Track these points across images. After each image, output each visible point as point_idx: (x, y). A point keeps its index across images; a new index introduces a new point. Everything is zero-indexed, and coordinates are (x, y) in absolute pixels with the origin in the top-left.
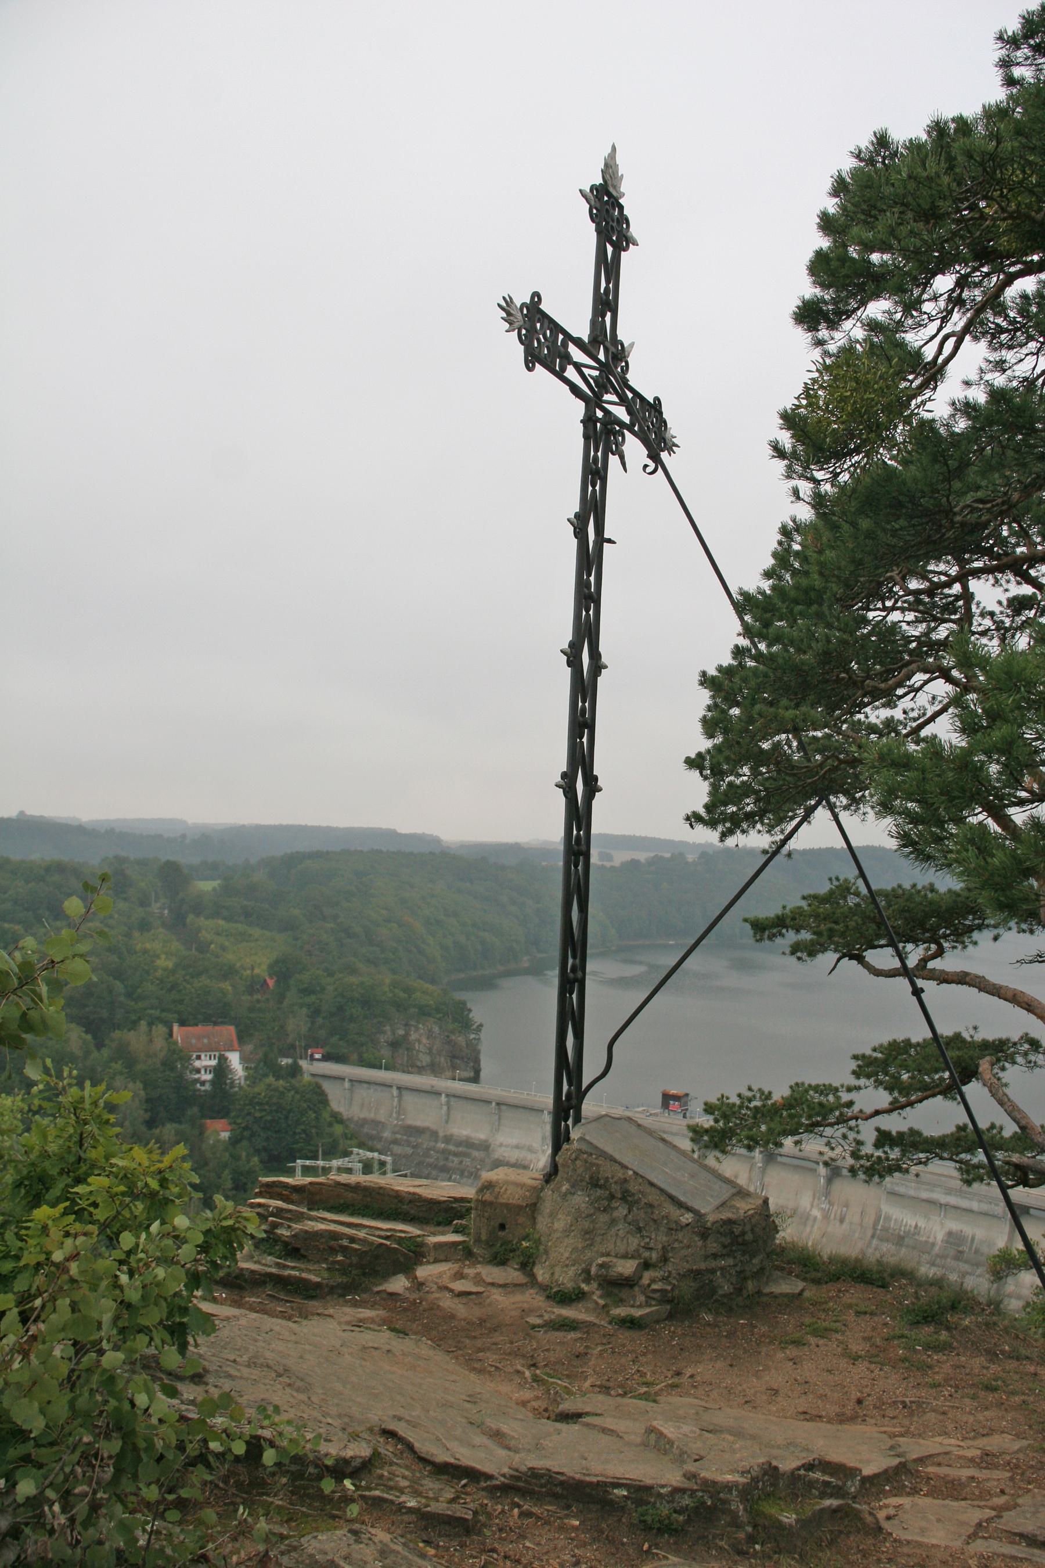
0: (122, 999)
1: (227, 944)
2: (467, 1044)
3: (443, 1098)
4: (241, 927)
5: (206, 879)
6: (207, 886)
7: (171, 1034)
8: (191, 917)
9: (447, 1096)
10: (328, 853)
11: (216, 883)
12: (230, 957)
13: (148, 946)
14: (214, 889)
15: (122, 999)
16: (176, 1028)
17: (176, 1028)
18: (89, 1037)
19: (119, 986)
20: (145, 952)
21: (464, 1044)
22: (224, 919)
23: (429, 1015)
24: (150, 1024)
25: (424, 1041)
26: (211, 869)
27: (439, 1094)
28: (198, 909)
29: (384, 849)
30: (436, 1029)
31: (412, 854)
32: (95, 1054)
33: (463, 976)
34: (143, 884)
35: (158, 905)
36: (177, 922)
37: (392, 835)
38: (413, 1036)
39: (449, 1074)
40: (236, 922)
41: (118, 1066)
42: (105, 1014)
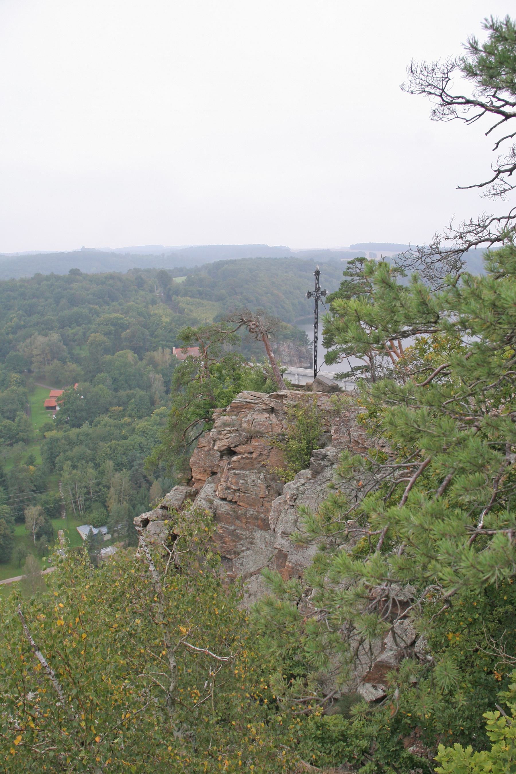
0: (149, 337)
1: (192, 309)
2: (306, 352)
3: (296, 376)
4: (198, 300)
5: (178, 277)
6: (179, 280)
7: (172, 352)
8: (174, 297)
9: (298, 375)
10: (235, 260)
11: (184, 278)
12: (194, 315)
13: (156, 312)
14: (183, 282)
15: (149, 337)
16: (174, 349)
17: (174, 349)
18: (136, 355)
19: (147, 332)
20: (156, 314)
21: (305, 351)
22: (190, 297)
23: (288, 338)
24: (163, 348)
25: (286, 350)
26: (181, 272)
27: (294, 374)
28: (177, 293)
29: (263, 257)
30: (292, 345)
31: (276, 259)
32: (140, 362)
33: (303, 318)
34: (150, 282)
35: (158, 291)
36: (168, 299)
37: (265, 248)
38: (281, 348)
39: (298, 365)
40: (196, 298)
41: (150, 367)
42: (141, 344)
